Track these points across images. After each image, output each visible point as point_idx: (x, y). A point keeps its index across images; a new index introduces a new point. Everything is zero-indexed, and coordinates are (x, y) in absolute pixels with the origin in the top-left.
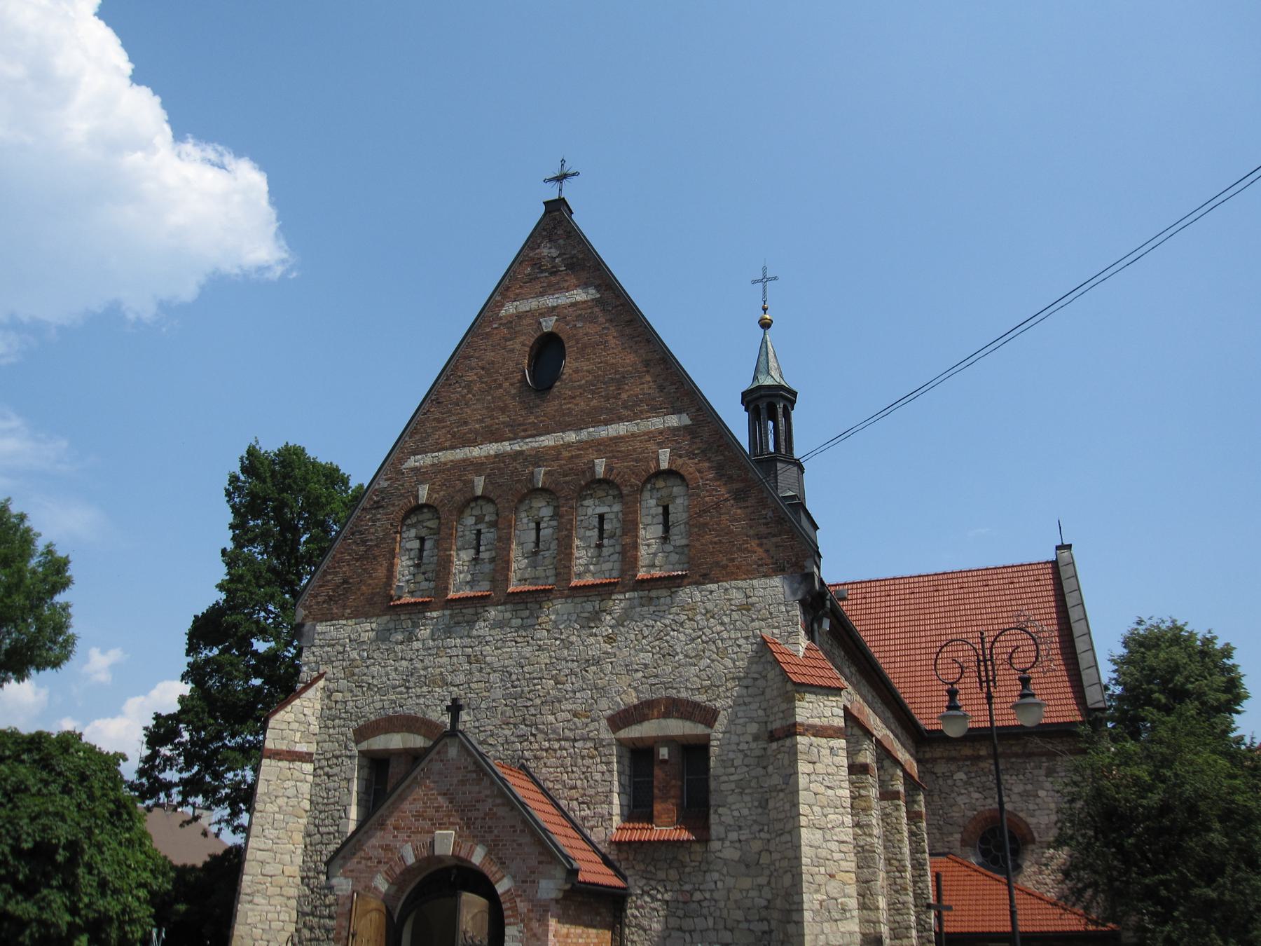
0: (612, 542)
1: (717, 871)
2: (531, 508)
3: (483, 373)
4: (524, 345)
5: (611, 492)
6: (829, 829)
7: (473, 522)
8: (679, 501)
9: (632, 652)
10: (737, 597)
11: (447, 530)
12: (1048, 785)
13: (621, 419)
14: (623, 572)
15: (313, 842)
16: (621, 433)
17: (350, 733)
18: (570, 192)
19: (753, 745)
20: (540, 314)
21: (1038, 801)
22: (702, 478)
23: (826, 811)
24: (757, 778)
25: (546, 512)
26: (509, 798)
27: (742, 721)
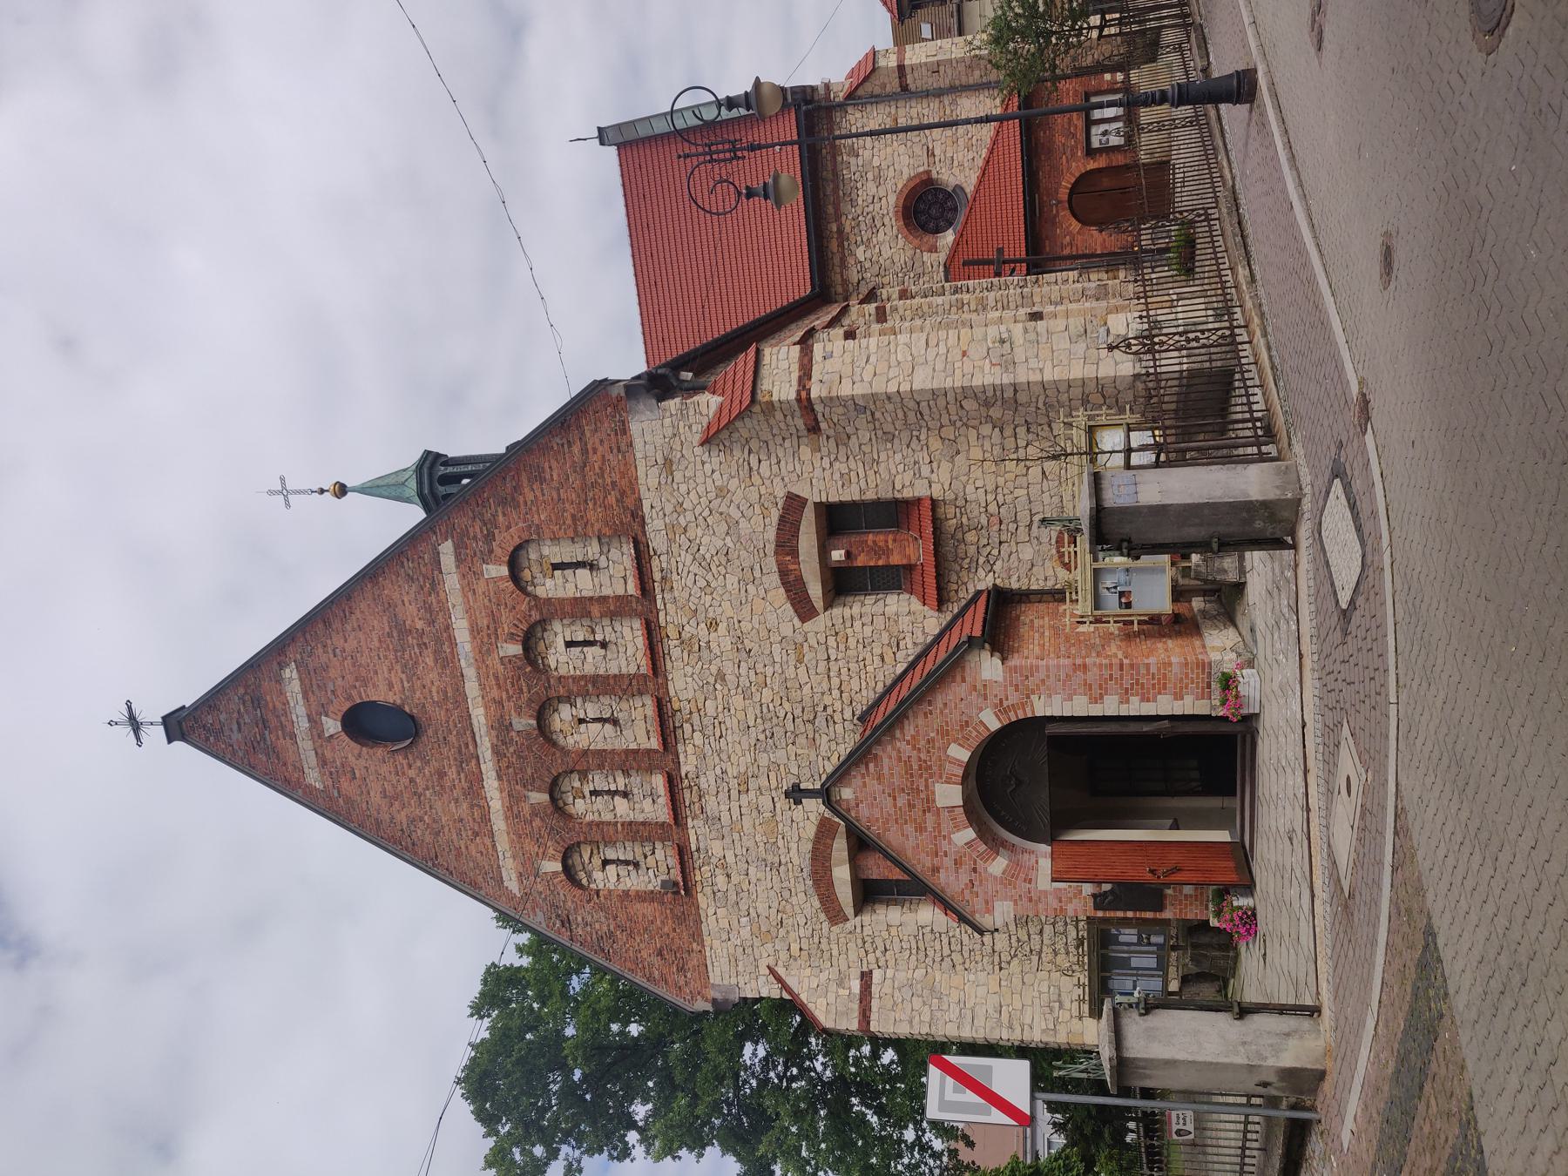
0: (598, 629)
1: (965, 487)
2: (561, 731)
4: (360, 756)
5: (539, 635)
6: (913, 360)
7: (581, 801)
8: (546, 551)
9: (725, 597)
12: (867, 154)
13: (448, 627)
14: (633, 614)
15: (961, 961)
18: (153, 710)
19: (824, 451)
20: (319, 737)
21: (884, 166)
22: (516, 524)
23: (894, 363)
24: (860, 445)
25: (565, 712)
27: (797, 466)
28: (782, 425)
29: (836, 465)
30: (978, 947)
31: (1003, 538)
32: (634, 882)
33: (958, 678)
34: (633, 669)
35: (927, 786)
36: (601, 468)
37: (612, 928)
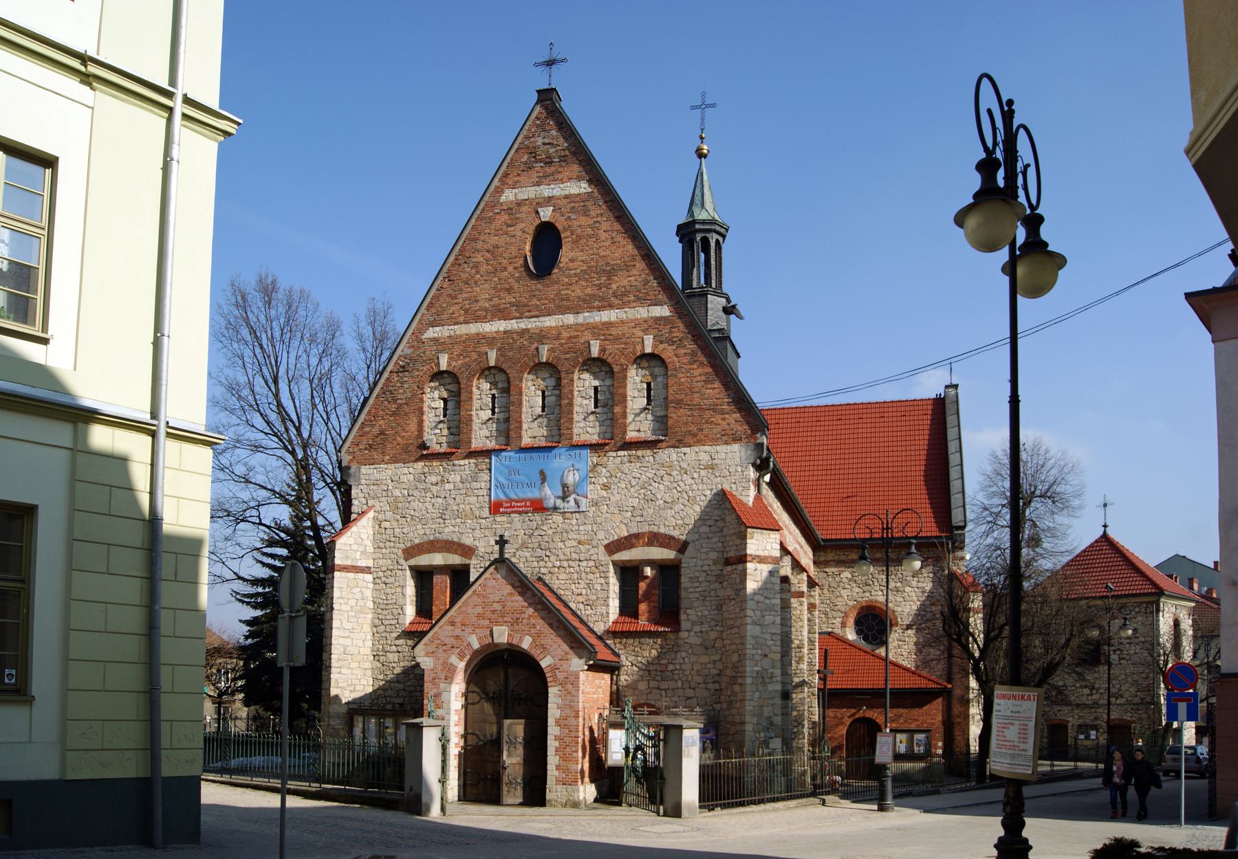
3: (489, 255)
5: (603, 369)
8: (660, 379)
10: (704, 457)
11: (466, 394)
13: (611, 306)
15: (379, 631)
16: (612, 319)
17: (400, 553)
19: (713, 568)
24: (715, 590)
26: (546, 605)
28: (731, 543)
29: (704, 574)
30: (389, 642)
31: (652, 673)
32: (430, 418)
33: (573, 645)
34: (575, 431)
35: (505, 622)
36: (712, 422)
37: (399, 401)
